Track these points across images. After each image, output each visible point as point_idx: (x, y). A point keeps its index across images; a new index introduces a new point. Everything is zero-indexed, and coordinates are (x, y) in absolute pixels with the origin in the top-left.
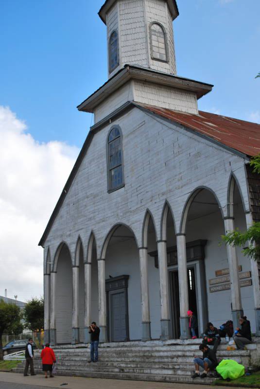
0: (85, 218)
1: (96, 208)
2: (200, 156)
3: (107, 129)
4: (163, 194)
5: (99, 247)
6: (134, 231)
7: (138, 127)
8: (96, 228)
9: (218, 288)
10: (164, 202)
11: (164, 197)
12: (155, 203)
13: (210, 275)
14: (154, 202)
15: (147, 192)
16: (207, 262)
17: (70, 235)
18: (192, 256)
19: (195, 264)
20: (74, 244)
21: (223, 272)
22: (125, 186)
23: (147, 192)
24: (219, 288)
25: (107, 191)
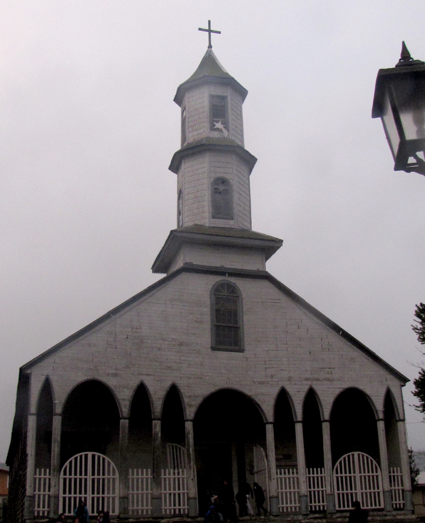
1: (183, 358)
2: (354, 362)
4: (307, 379)
5: (190, 406)
6: (260, 403)
7: (270, 301)
8: (181, 382)
11: (309, 383)
12: (295, 384)
14: (293, 382)
15: (282, 370)
17: (115, 375)
20: (127, 388)
22: (245, 352)
23: (282, 370)
25: (209, 346)
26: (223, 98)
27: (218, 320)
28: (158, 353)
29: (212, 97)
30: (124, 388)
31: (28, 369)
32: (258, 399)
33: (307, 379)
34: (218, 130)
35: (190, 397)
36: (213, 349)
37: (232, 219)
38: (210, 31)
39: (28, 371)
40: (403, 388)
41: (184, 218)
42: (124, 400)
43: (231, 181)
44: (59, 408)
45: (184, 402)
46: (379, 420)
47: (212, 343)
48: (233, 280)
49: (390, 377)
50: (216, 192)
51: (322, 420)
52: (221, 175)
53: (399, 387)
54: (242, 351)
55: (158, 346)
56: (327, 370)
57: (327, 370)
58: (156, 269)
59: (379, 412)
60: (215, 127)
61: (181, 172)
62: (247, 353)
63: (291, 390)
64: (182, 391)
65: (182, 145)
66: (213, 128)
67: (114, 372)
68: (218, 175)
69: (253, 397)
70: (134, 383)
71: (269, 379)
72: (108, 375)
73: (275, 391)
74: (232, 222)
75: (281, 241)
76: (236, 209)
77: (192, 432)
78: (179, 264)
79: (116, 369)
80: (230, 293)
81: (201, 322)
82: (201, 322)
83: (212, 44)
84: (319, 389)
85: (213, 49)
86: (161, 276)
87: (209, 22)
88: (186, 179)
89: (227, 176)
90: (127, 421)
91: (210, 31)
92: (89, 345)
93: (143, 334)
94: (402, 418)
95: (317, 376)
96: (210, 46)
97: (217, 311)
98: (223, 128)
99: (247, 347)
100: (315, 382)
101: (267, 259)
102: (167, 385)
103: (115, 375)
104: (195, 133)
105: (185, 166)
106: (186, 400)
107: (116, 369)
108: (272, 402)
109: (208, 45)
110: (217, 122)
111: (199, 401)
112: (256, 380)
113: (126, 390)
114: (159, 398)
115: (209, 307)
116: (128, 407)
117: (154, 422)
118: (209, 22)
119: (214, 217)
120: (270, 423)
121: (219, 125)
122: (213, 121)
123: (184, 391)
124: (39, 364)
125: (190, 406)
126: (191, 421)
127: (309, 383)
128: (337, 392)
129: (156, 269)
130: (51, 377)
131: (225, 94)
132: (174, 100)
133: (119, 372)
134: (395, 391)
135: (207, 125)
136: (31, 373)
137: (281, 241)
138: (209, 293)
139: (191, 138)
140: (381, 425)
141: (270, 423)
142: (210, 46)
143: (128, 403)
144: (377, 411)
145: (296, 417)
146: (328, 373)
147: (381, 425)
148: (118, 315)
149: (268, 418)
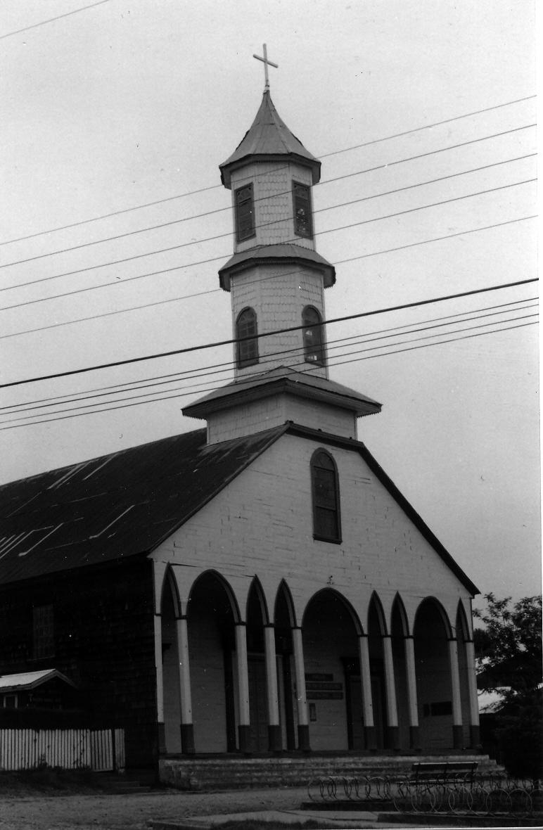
38: (265, 61)
43: (321, 312)
48: (330, 449)
49: (461, 586)
53: (469, 600)
58: (189, 411)
87: (265, 46)
91: (265, 61)
118: (265, 46)
136: (152, 559)
140: (454, 646)
147: (454, 646)
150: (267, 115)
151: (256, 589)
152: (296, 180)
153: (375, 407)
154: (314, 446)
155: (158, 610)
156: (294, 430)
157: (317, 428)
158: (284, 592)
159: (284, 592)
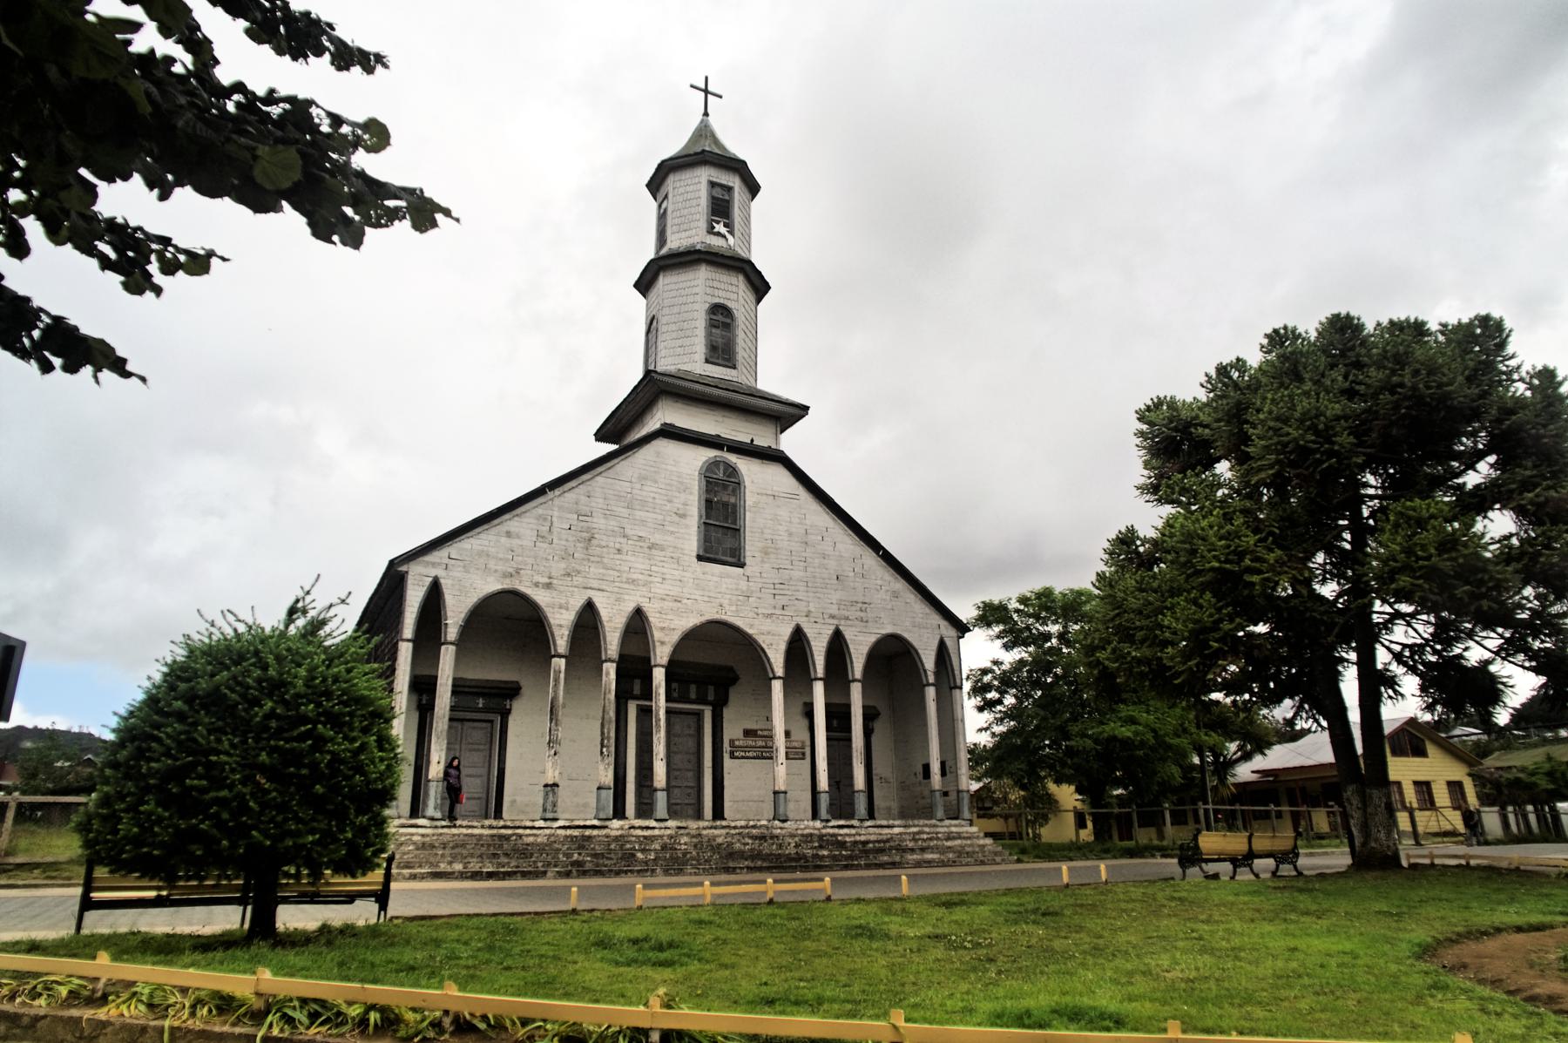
0: (616, 574)
3: (711, 454)
4: (832, 617)
5: (662, 643)
6: (764, 646)
9: (747, 754)
10: (833, 628)
11: (836, 622)
13: (731, 732)
16: (727, 713)
18: (675, 695)
19: (703, 710)
20: (567, 609)
21: (760, 733)
24: (751, 754)
25: (695, 554)
26: (729, 189)
27: (708, 517)
28: (618, 556)
29: (713, 184)
30: (561, 607)
31: (402, 565)
32: (762, 640)
33: (832, 617)
34: (719, 234)
35: (663, 629)
36: (700, 558)
37: (734, 367)
38: (706, 91)
39: (403, 568)
40: (961, 640)
41: (658, 359)
42: (561, 626)
44: (452, 633)
45: (652, 636)
46: (929, 684)
47: (698, 549)
48: (733, 458)
49: (944, 623)
50: (712, 324)
51: (851, 678)
52: (722, 301)
54: (742, 565)
55: (617, 546)
56: (860, 605)
57: (860, 605)
58: (601, 435)
59: (929, 673)
60: (716, 230)
61: (653, 293)
62: (748, 570)
63: (809, 631)
64: (650, 619)
65: (657, 252)
66: (711, 230)
67: (547, 580)
68: (717, 300)
69: (756, 637)
70: (577, 603)
71: (779, 612)
72: (537, 585)
73: (786, 631)
74: (733, 372)
75: (808, 408)
76: (741, 354)
77: (663, 684)
78: (653, 424)
79: (550, 578)
80: (728, 476)
81: (683, 516)
82: (683, 516)
83: (709, 111)
84: (849, 634)
85: (710, 118)
86: (608, 447)
87: (707, 78)
88: (665, 301)
89: (729, 304)
90: (563, 660)
91: (706, 91)
92: (509, 534)
93: (595, 526)
94: (958, 684)
95: (846, 613)
96: (706, 114)
97: (709, 502)
98: (727, 234)
99: (748, 561)
100: (843, 622)
101: (782, 432)
102: (629, 607)
103: (548, 586)
104: (683, 235)
105: (666, 283)
106: (657, 635)
107: (550, 578)
108: (783, 647)
109: (702, 111)
110: (718, 222)
111: (675, 637)
112: (760, 611)
113: (564, 611)
114: (616, 628)
115: (696, 493)
116: (565, 638)
117: (605, 665)
118: (707, 78)
119: (707, 361)
120: (779, 678)
121: (720, 228)
122: (713, 220)
123: (654, 619)
124: (421, 559)
125: (662, 643)
126: (662, 666)
127: (836, 622)
128: (873, 639)
129: (601, 435)
130: (442, 581)
131: (731, 184)
132: (647, 186)
133: (555, 581)
134: (949, 643)
135: (703, 225)
136: (407, 572)
137: (808, 408)
138: (697, 473)
139: (675, 242)
140: (931, 693)
141: (779, 678)
142: (706, 114)
143: (567, 633)
144: (925, 671)
145: (815, 671)
146: (861, 610)
147: (931, 693)
148: (557, 492)
149: (776, 669)
150: (704, 131)
151: (589, 612)
152: (711, 179)
153: (803, 410)
154: (707, 454)
155: (408, 630)
156: (669, 433)
157: (713, 433)
158: (638, 624)
159: (638, 624)
